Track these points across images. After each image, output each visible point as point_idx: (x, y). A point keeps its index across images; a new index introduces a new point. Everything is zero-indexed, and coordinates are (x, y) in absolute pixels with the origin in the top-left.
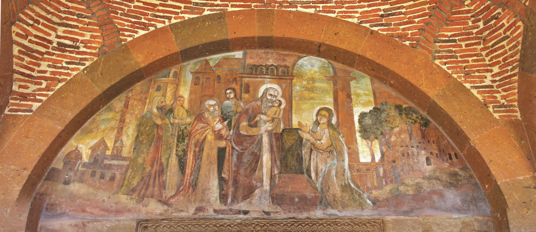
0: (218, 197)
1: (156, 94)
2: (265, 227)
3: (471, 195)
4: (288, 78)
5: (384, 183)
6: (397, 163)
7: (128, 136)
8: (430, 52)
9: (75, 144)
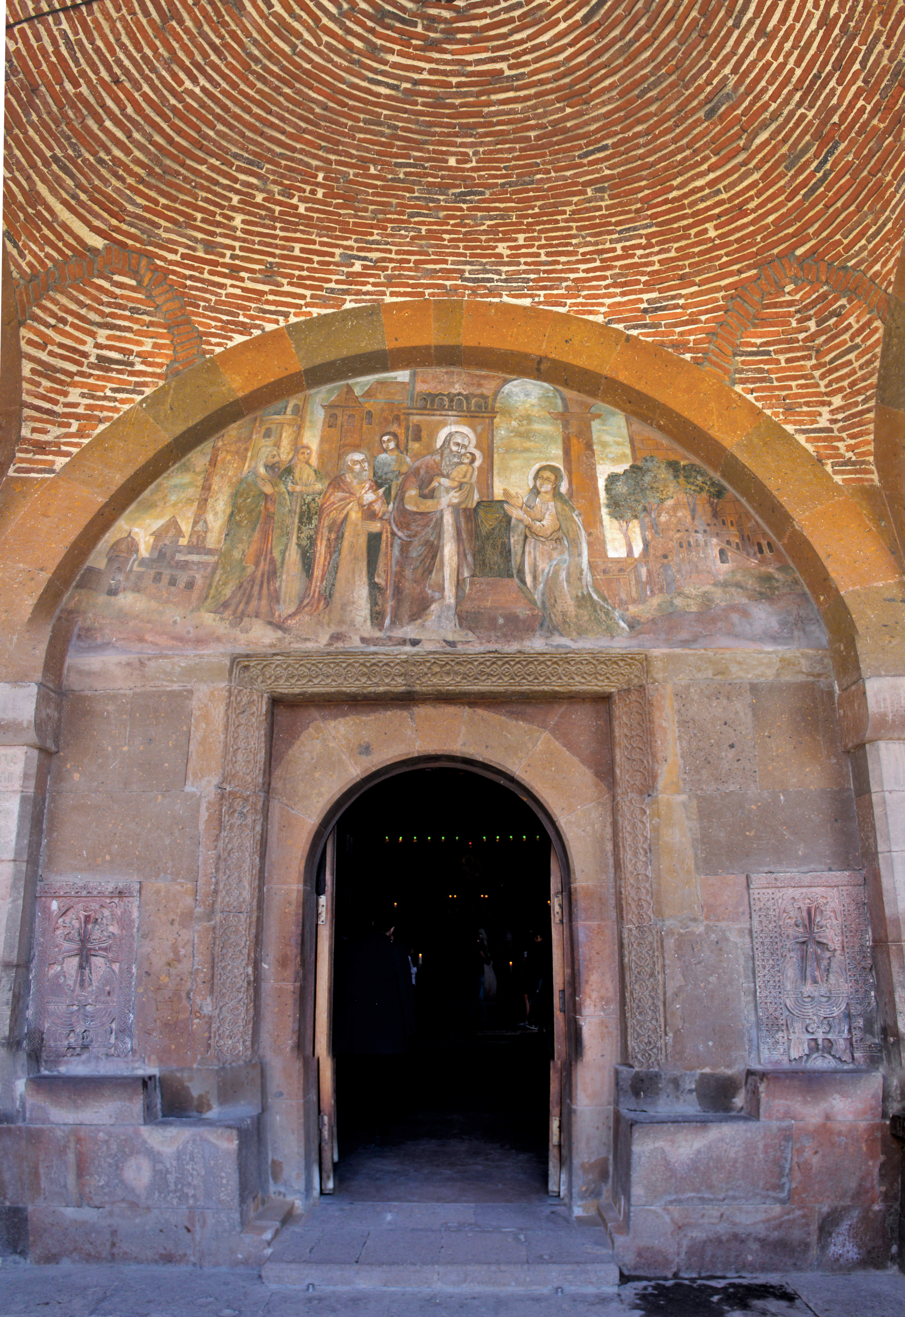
2: (448, 667)
3: (795, 612)
7: (216, 514)
8: (726, 371)
9: (126, 527)
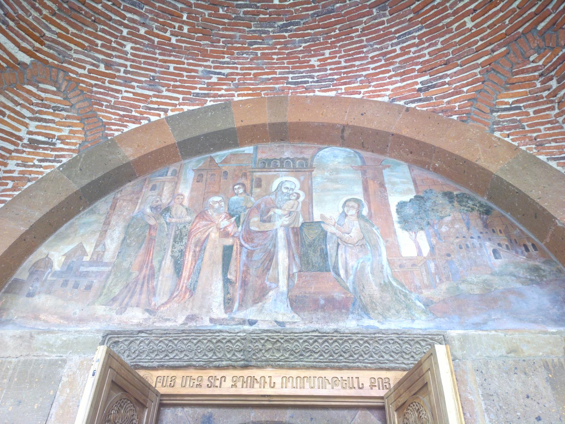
0: (222, 302)
1: (150, 193)
4: (306, 170)
5: (438, 281)
6: (452, 256)
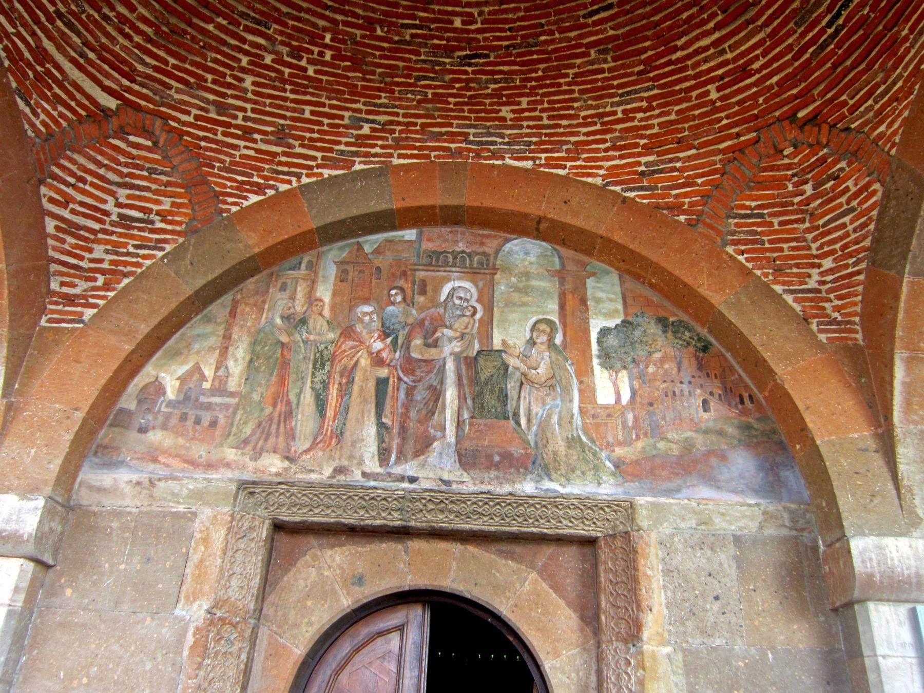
0: (376, 453)
1: (280, 295)
4: (487, 271)
5: (634, 437)
6: (655, 406)
7: (236, 360)
